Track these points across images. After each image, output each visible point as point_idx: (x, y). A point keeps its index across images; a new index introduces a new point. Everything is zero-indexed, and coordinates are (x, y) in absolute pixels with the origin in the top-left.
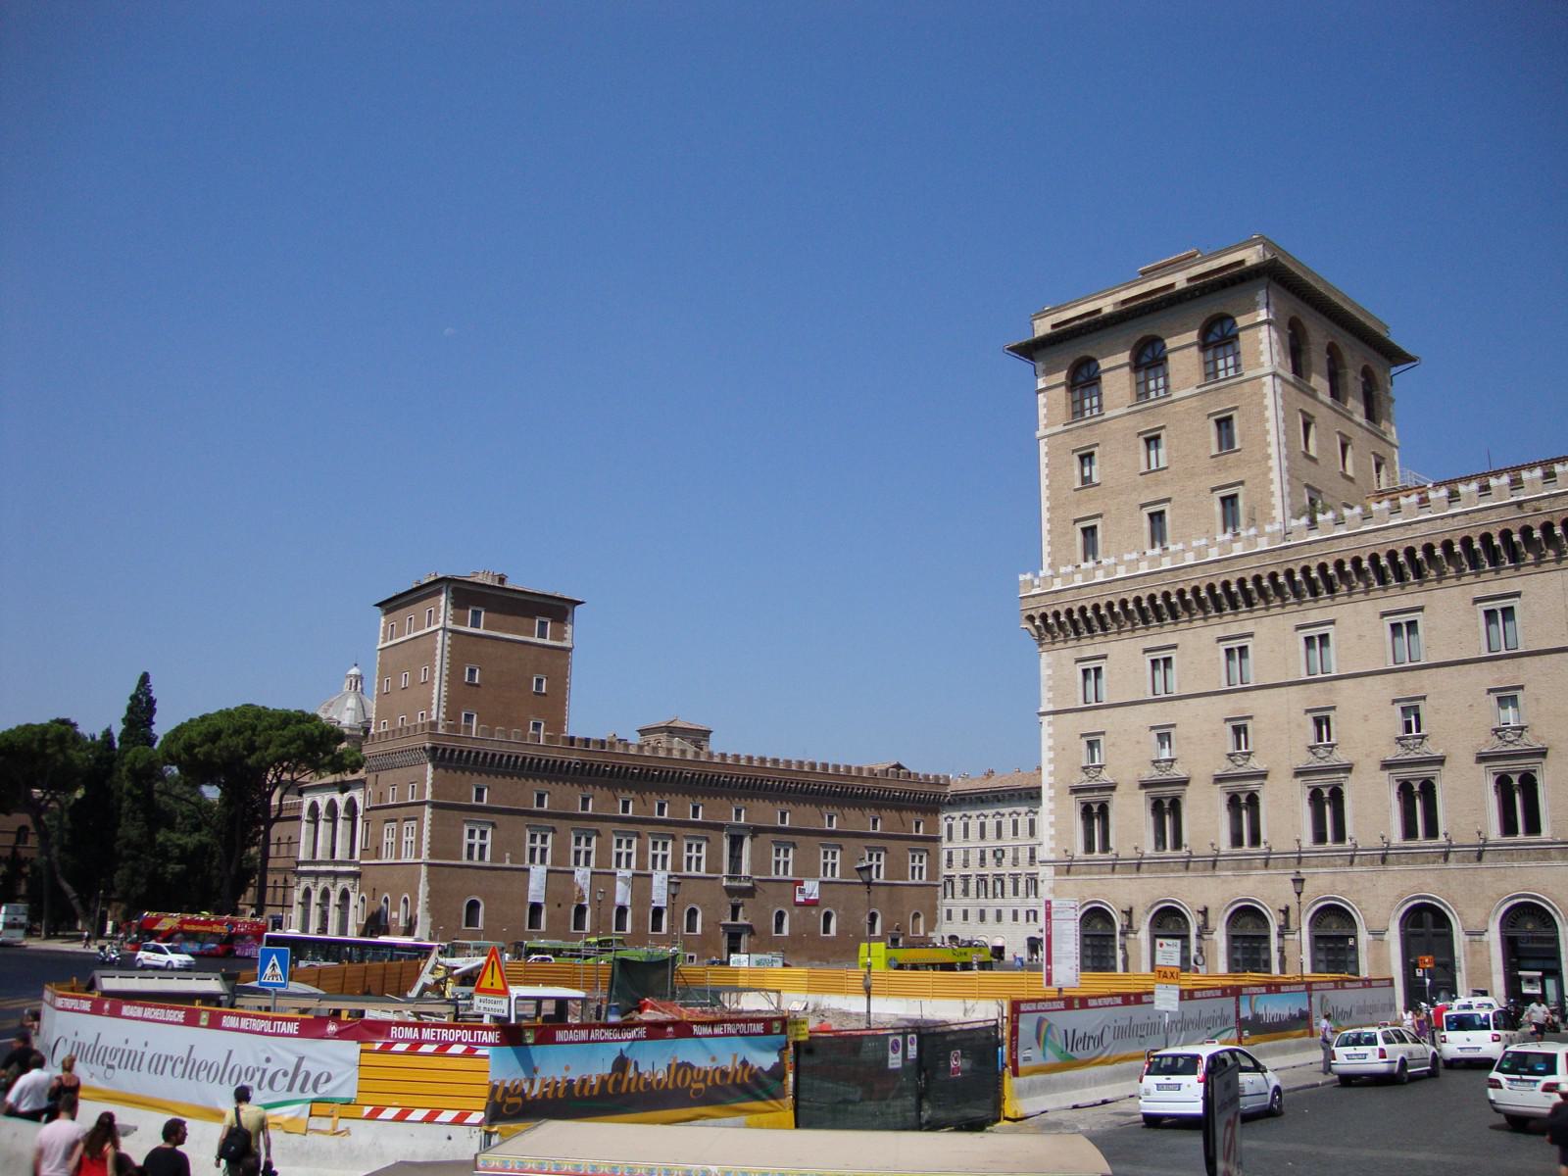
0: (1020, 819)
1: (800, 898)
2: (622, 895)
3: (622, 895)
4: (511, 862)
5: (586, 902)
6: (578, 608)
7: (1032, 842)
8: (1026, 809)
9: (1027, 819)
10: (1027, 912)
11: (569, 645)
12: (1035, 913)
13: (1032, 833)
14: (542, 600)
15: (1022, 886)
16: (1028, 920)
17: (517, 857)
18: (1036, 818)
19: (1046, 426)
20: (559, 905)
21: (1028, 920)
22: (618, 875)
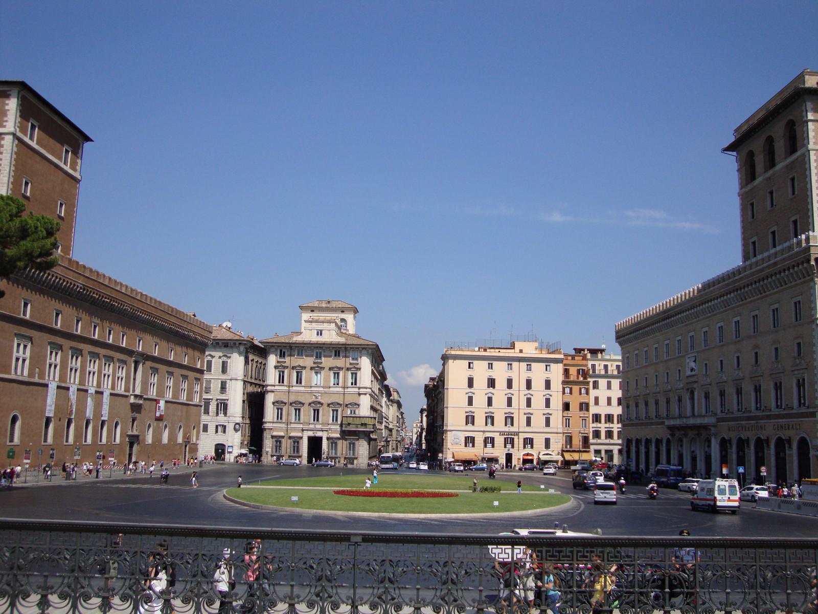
0: (214, 360)
1: (158, 414)
2: (89, 413)
3: (89, 413)
4: (39, 378)
5: (73, 417)
6: (87, 145)
7: (224, 377)
8: (221, 354)
9: (221, 361)
10: (217, 427)
11: (79, 177)
12: (224, 427)
13: (224, 370)
14: (68, 129)
15: (212, 407)
16: (217, 432)
17: (42, 375)
18: (229, 361)
19: (815, 143)
20: (60, 420)
21: (217, 432)
22: (89, 392)
